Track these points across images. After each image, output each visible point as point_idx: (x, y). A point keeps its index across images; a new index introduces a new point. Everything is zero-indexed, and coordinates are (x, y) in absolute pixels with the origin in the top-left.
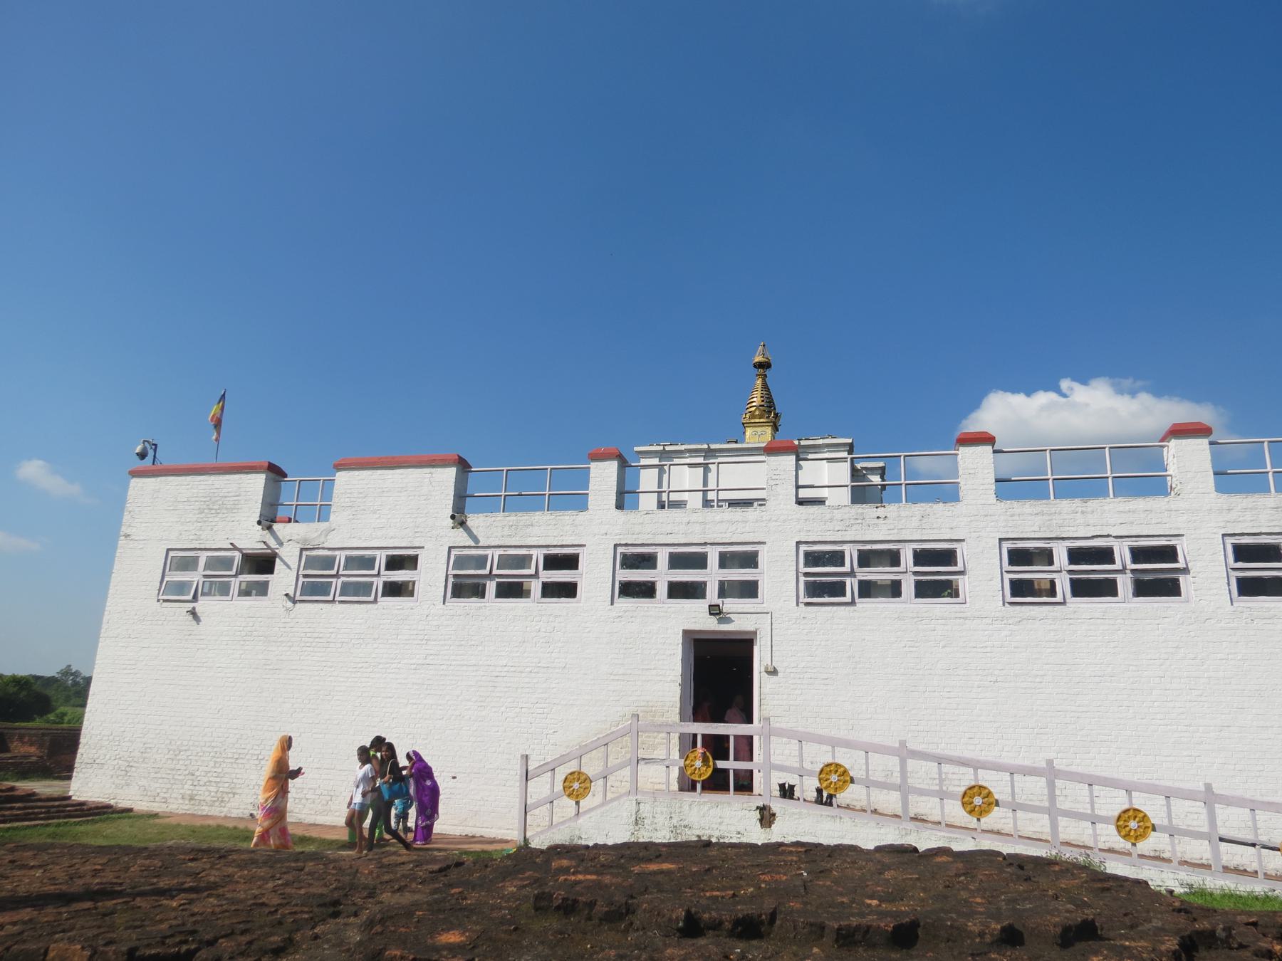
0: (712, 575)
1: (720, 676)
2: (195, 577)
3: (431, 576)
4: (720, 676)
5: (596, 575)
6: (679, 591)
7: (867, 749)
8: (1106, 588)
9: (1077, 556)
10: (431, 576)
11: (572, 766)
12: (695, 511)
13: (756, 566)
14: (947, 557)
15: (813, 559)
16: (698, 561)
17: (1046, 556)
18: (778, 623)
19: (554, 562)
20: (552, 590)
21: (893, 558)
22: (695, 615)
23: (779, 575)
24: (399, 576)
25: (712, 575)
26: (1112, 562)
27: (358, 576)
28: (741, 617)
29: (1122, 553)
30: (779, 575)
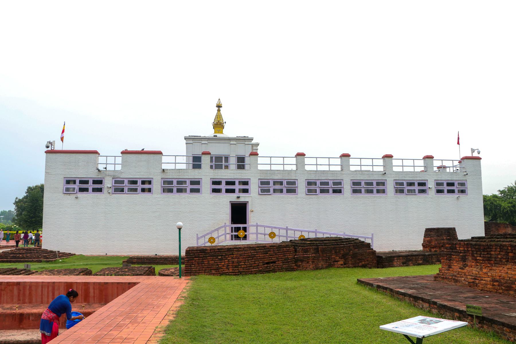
0: (237, 187)
1: (239, 213)
4: (239, 213)
6: (228, 191)
7: (279, 229)
8: (327, 191)
9: (322, 184)
11: (209, 236)
12: (232, 170)
13: (248, 184)
14: (294, 183)
15: (262, 183)
16: (233, 183)
17: (315, 184)
18: (254, 200)
19: (192, 183)
20: (192, 191)
21: (281, 183)
22: (233, 197)
24: (146, 186)
25: (237, 187)
26: (329, 185)
27: (133, 186)
29: (331, 183)
30: (254, 187)
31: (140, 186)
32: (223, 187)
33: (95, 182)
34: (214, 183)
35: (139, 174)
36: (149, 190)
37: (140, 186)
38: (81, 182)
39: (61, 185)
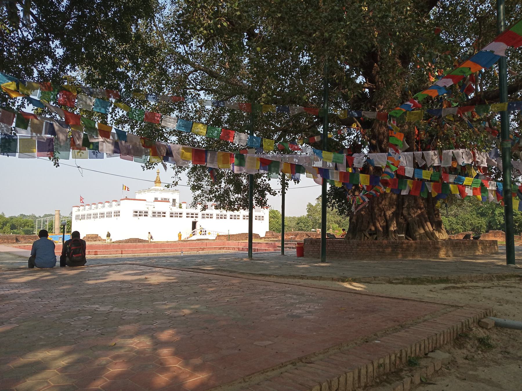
0: (194, 216)
2: (138, 214)
3: (168, 215)
5: (184, 215)
10: (168, 215)
16: (193, 214)
19: (180, 214)
20: (180, 217)
22: (193, 219)
23: (200, 215)
25: (194, 216)
27: (159, 214)
28: (197, 219)
30: (200, 215)
31: (162, 214)
32: (190, 215)
33: (145, 212)
34: (187, 214)
35: (162, 210)
36: (164, 216)
37: (162, 214)
38: (140, 212)
39: (132, 214)
